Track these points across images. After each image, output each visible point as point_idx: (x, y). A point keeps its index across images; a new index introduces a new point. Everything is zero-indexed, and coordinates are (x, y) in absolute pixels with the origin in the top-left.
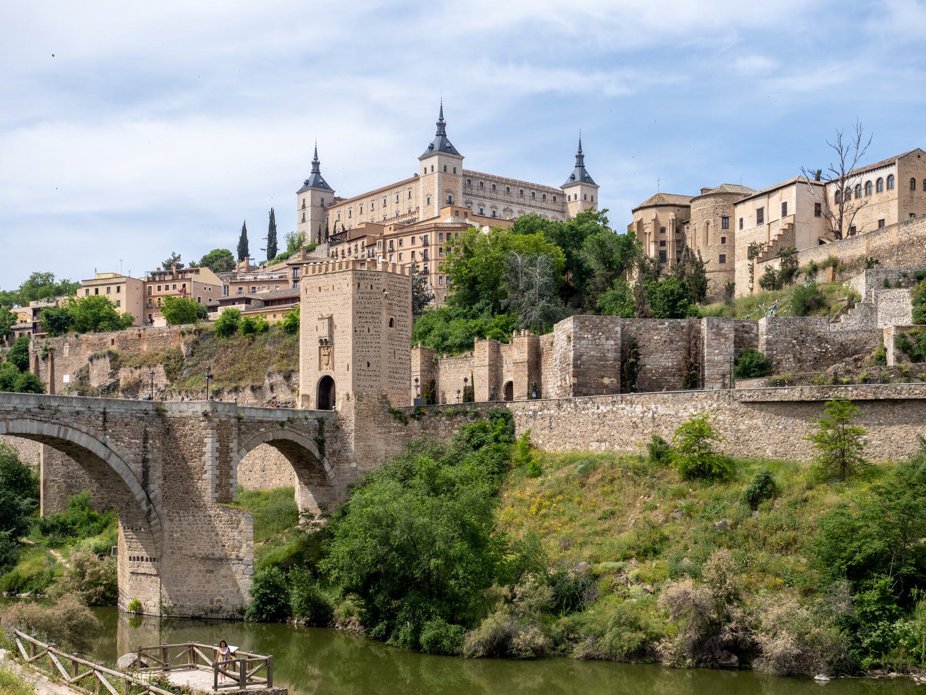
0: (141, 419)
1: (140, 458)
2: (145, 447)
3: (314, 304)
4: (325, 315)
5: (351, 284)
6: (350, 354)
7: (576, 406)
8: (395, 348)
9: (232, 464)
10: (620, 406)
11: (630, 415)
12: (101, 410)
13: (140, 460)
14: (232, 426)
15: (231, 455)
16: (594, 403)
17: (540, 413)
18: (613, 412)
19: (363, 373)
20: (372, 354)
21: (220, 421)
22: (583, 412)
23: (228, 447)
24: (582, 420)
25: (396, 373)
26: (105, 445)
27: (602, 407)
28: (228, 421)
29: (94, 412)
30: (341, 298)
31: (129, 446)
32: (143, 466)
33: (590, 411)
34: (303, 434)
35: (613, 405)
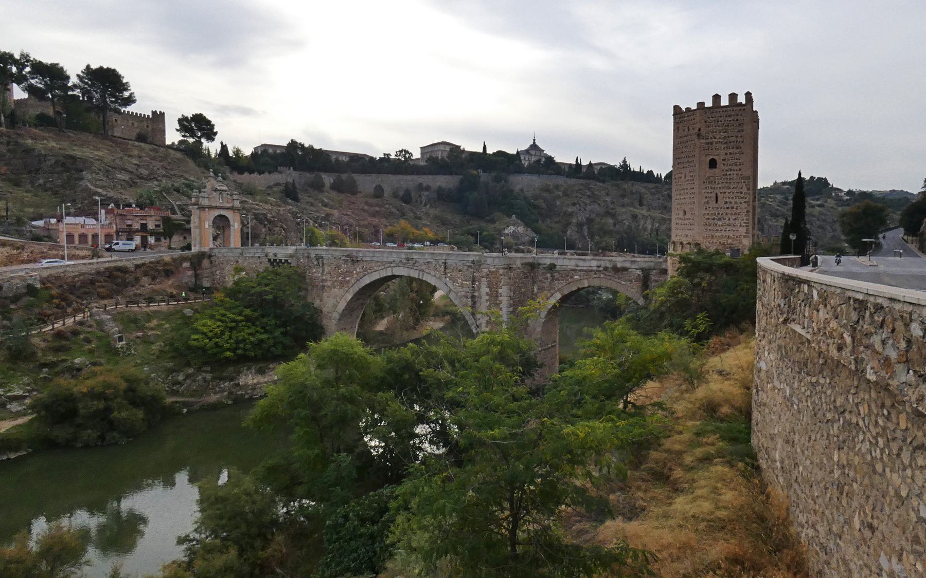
0: (470, 267)
1: (470, 295)
2: (473, 287)
8: (716, 191)
9: (501, 306)
12: (443, 261)
13: (469, 296)
14: (501, 275)
15: (500, 298)
19: (680, 222)
20: (688, 201)
21: (490, 271)
23: (497, 292)
25: (719, 219)
26: (446, 284)
28: (497, 271)
29: (438, 262)
31: (462, 286)
32: (472, 301)
34: (623, 283)
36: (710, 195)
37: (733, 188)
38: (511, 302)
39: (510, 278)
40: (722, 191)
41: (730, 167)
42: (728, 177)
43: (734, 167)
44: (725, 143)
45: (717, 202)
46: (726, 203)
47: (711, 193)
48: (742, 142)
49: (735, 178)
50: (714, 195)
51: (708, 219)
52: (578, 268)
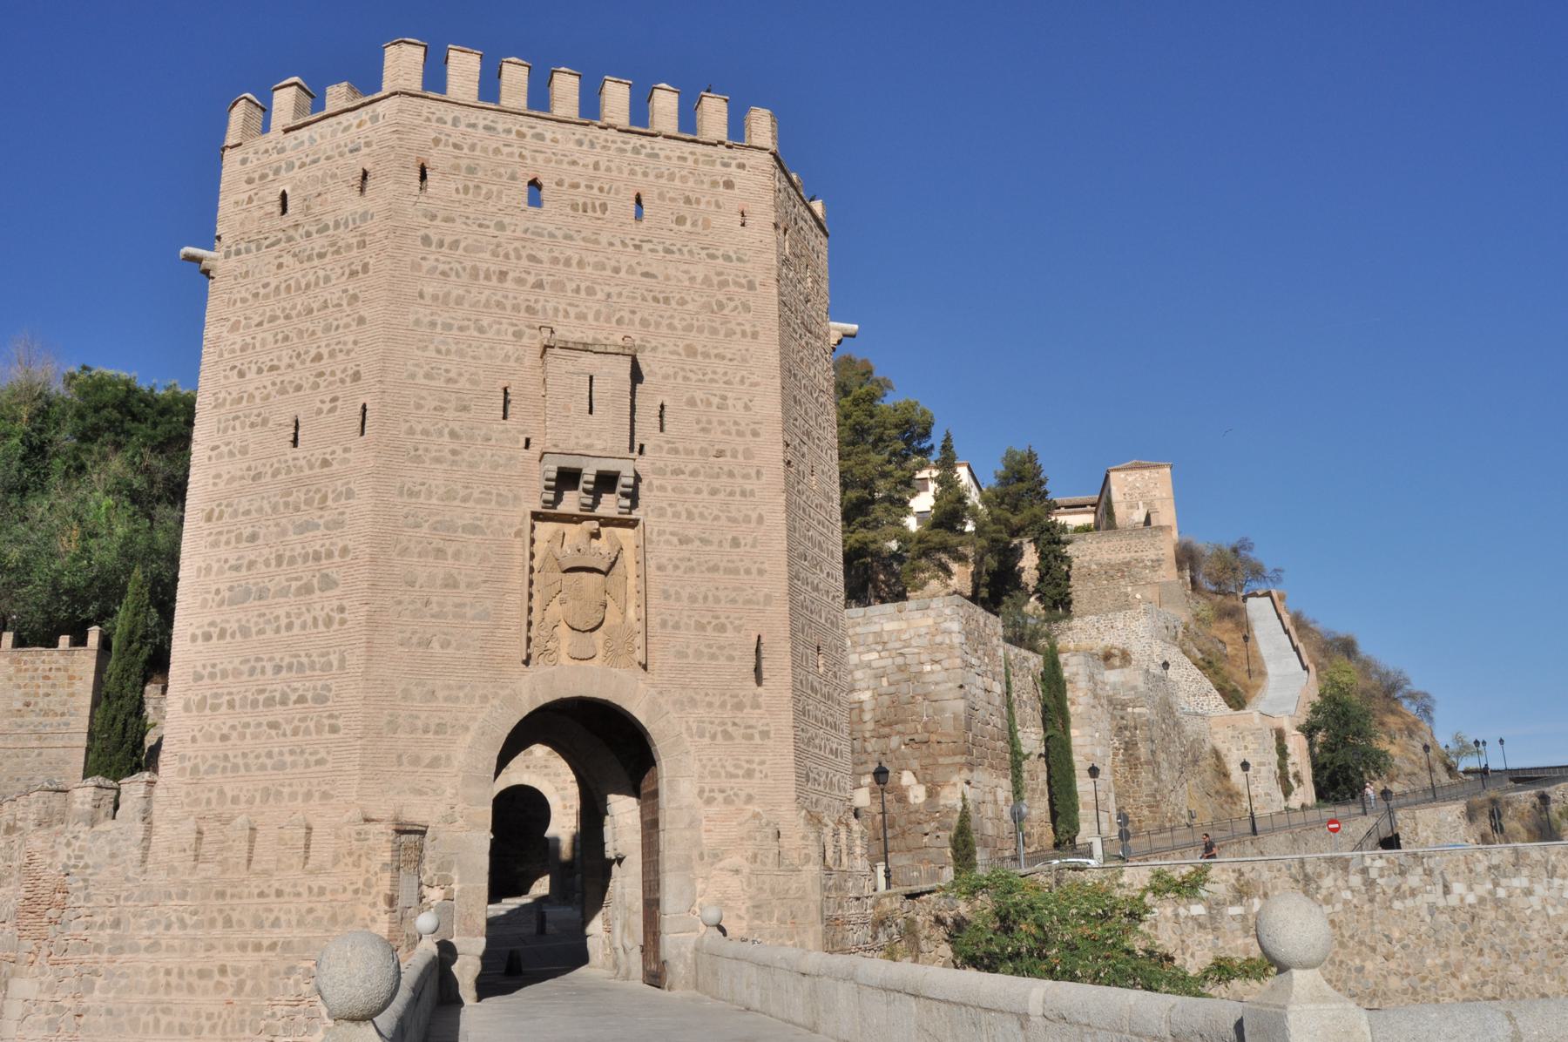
3: (486, 261)
4: (569, 331)
5: (764, 214)
6: (777, 582)
7: (1370, 884)
10: (1516, 882)
11: (1551, 912)
16: (1429, 873)
17: (1236, 910)
18: (1498, 904)
22: (1397, 905)
24: (1396, 934)
27: (1458, 888)
30: (699, 272)
33: (1422, 901)
35: (1496, 885)
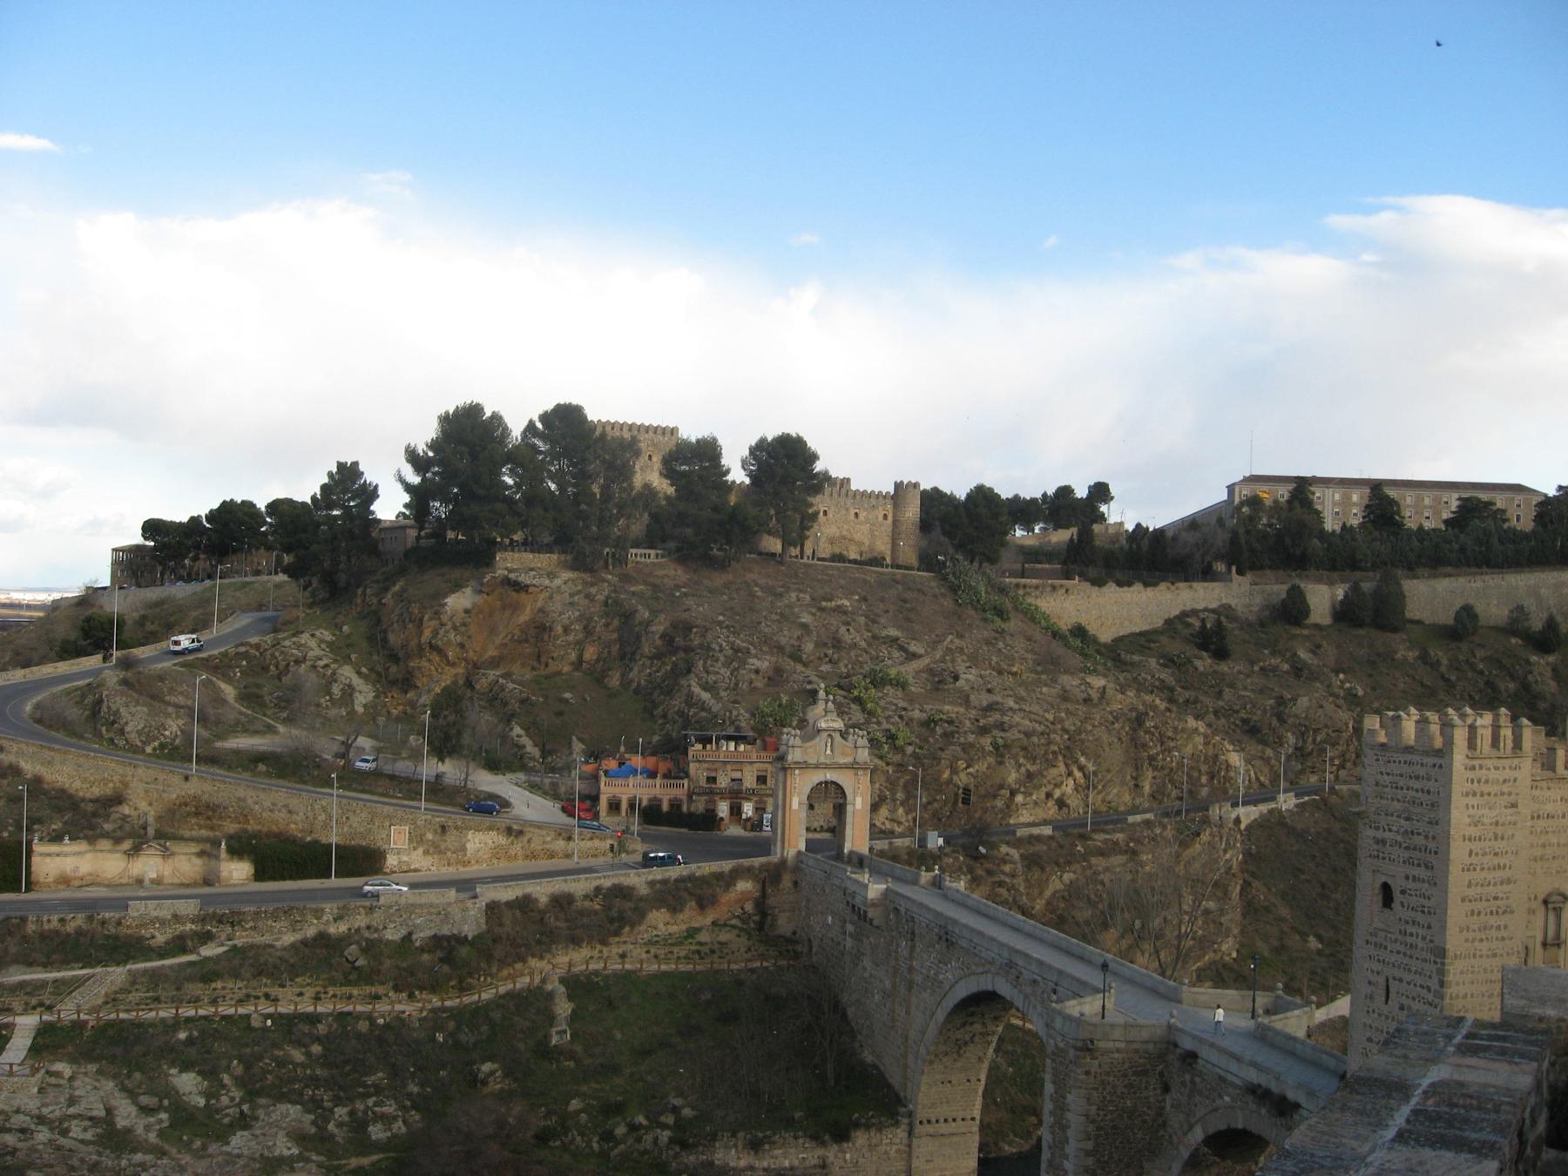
36: (1374, 978)
37: (1416, 972)
38: (1091, 1128)
39: (1088, 1073)
40: (1398, 973)
41: (1412, 914)
42: (1409, 940)
43: (1420, 917)
44: (1406, 848)
45: (1386, 1003)
46: (1402, 1008)
47: (1378, 973)
48: (1436, 853)
49: (1420, 945)
50: (1382, 981)
51: (1369, 1040)
52: (1230, 1078)
